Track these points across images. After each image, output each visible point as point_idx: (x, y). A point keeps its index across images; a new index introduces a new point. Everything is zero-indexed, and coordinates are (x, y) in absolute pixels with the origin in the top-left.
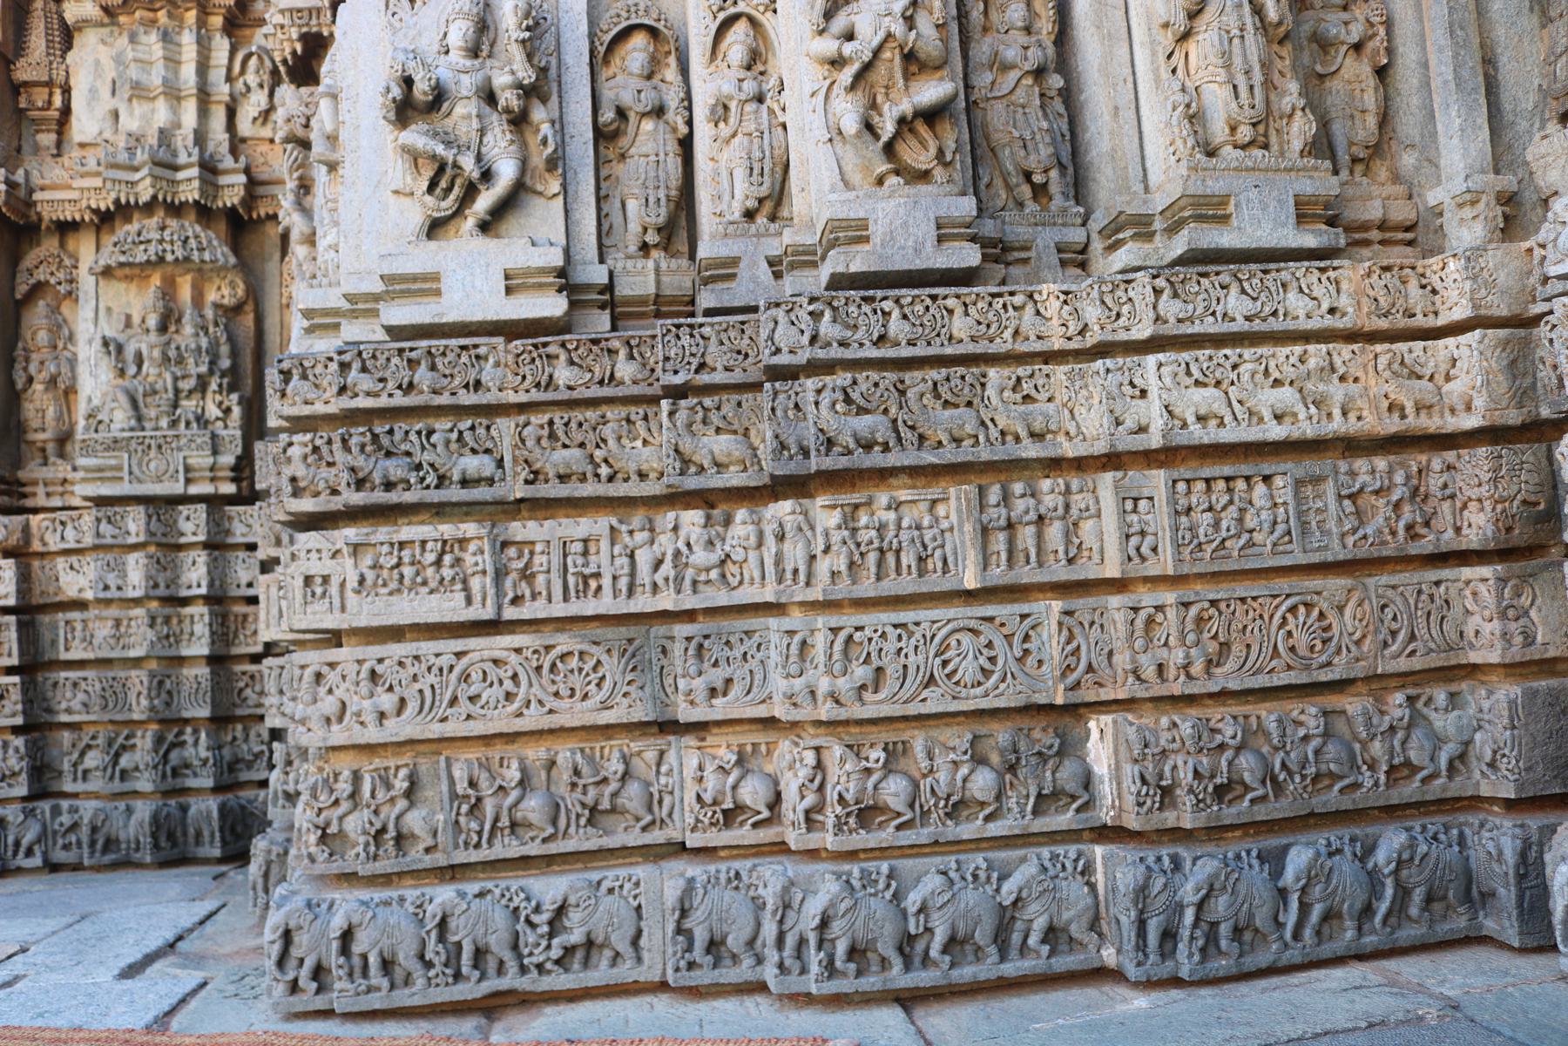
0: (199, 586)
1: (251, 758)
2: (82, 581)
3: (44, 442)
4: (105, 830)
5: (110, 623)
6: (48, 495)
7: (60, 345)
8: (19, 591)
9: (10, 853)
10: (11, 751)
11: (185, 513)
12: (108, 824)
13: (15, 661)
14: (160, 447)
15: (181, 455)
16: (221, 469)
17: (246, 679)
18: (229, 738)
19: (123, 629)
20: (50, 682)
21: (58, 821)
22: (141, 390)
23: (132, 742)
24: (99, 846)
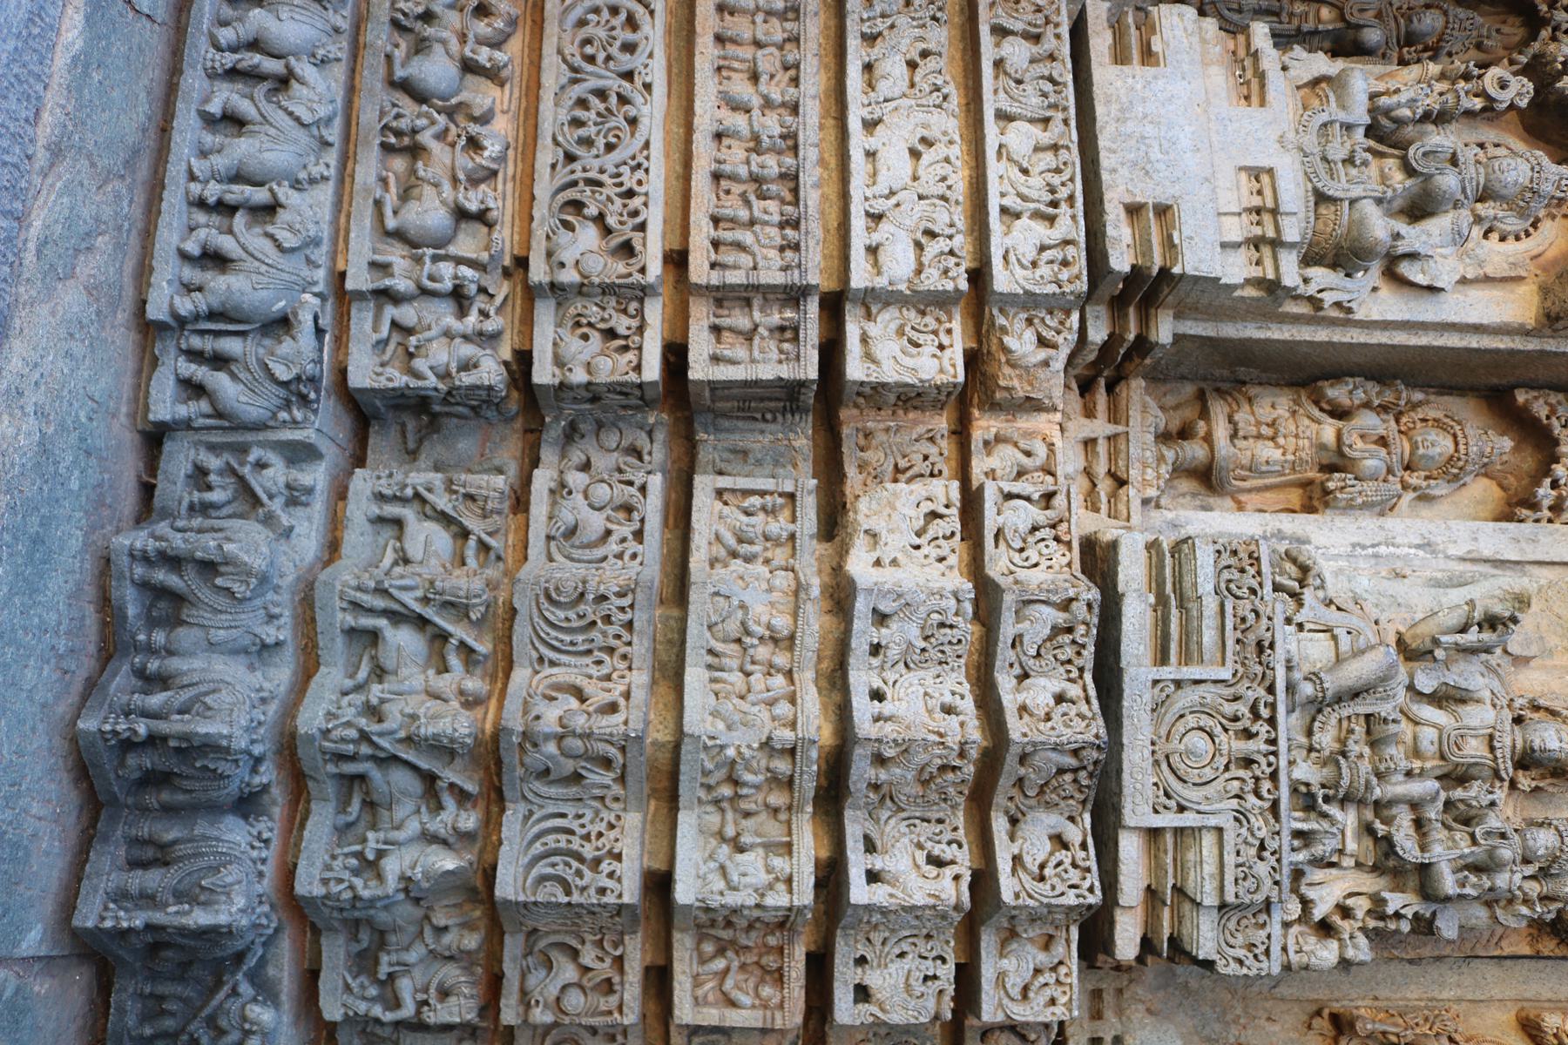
0: (873, 877)
1: (383, 971)
2: (896, 542)
3: (1208, 439)
4: (205, 594)
5: (782, 623)
6: (1089, 443)
7: (1414, 479)
8: (879, 388)
9: (196, 342)
10: (467, 350)
11: (1074, 834)
12: (222, 602)
13: (699, 369)
14: (1248, 762)
15: (1226, 822)
16: (1178, 919)
17: (605, 969)
18: (440, 919)
19: (763, 652)
20: (642, 440)
21: (271, 457)
22: (1385, 709)
23: (454, 661)
24: (161, 576)
